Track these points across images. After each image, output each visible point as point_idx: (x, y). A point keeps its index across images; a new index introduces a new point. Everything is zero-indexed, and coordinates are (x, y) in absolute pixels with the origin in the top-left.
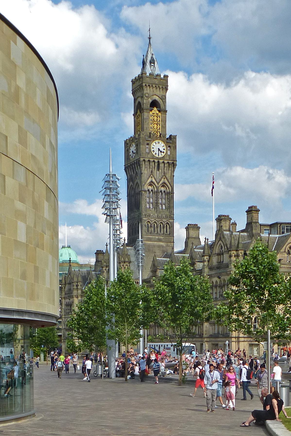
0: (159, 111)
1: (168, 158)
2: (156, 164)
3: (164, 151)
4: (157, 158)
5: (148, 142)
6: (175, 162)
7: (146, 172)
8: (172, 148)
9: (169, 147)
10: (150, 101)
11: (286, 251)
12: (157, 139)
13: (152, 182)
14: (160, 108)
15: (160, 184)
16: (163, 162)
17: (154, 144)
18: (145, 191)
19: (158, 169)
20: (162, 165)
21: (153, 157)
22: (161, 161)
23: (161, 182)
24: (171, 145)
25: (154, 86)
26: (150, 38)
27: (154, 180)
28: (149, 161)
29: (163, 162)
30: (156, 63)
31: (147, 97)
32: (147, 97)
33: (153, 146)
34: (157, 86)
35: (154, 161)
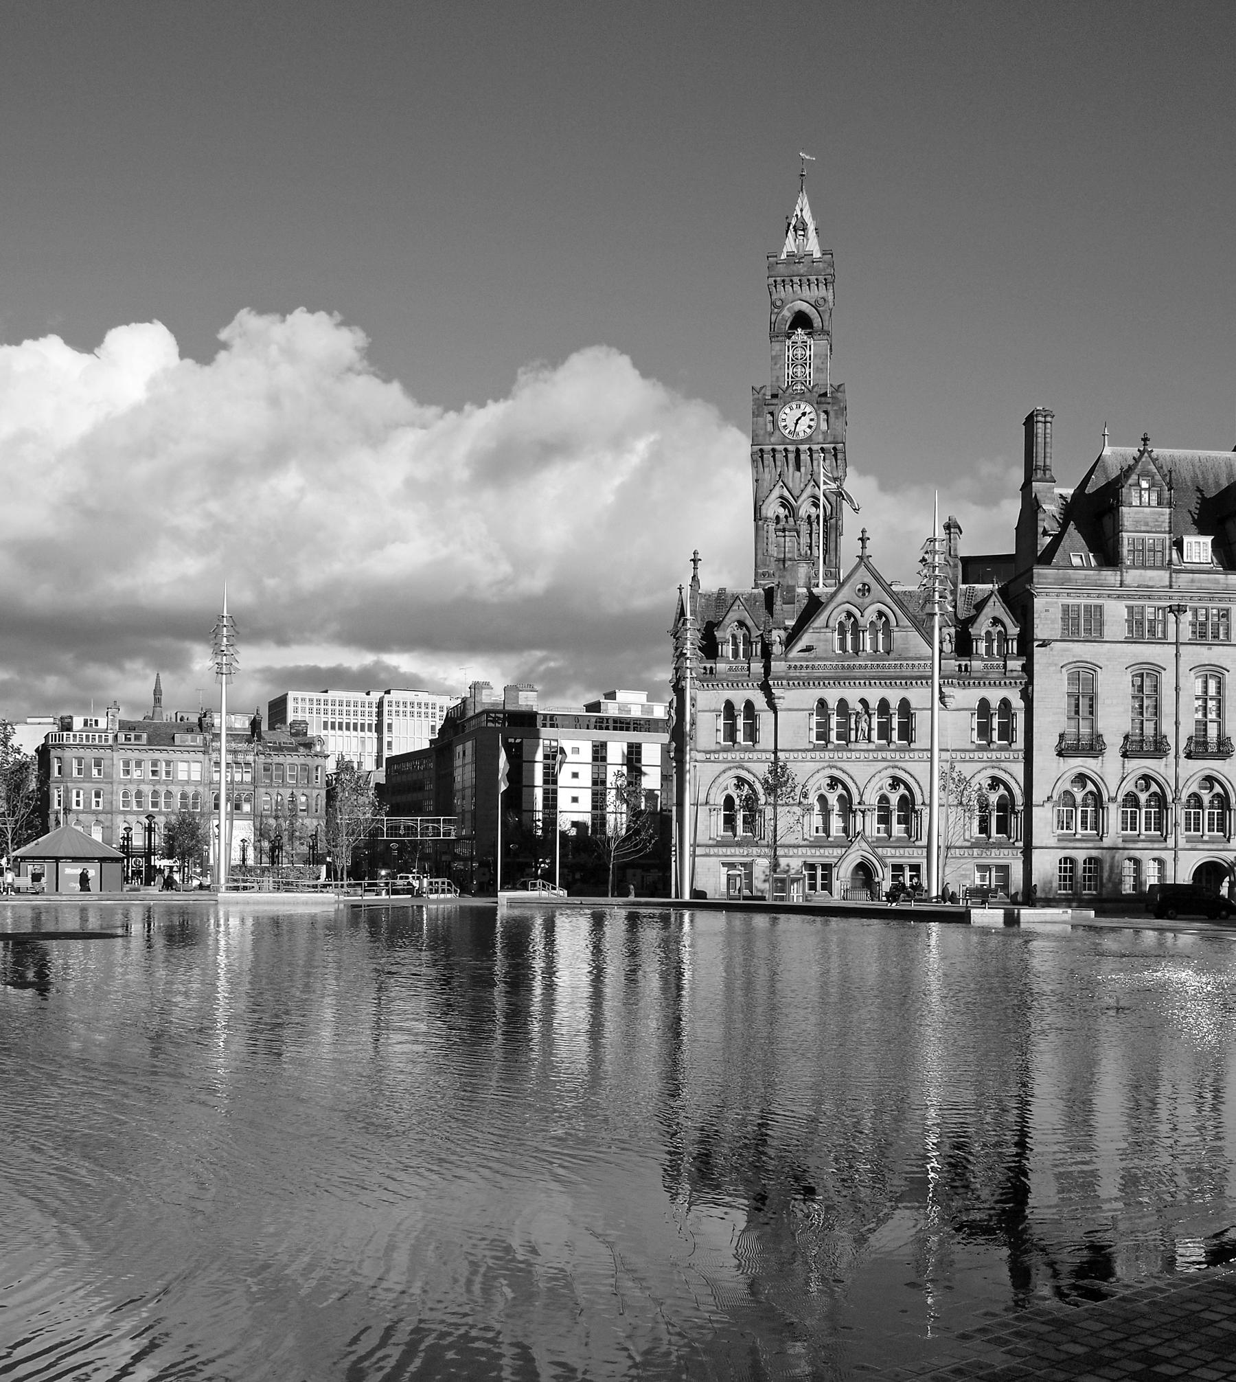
1: (820, 438)
2: (791, 456)
3: (812, 423)
4: (793, 442)
5: (771, 408)
7: (767, 476)
8: (832, 414)
9: (826, 412)
10: (787, 314)
11: (834, 623)
12: (793, 399)
13: (782, 497)
14: (812, 327)
16: (810, 449)
17: (787, 410)
18: (766, 519)
19: (798, 469)
20: (805, 457)
22: (804, 447)
23: (805, 495)
24: (829, 408)
25: (796, 279)
27: (786, 494)
28: (774, 450)
29: (810, 449)
30: (811, 228)
31: (778, 307)
32: (778, 307)
33: (784, 416)
34: (804, 279)
35: (786, 450)
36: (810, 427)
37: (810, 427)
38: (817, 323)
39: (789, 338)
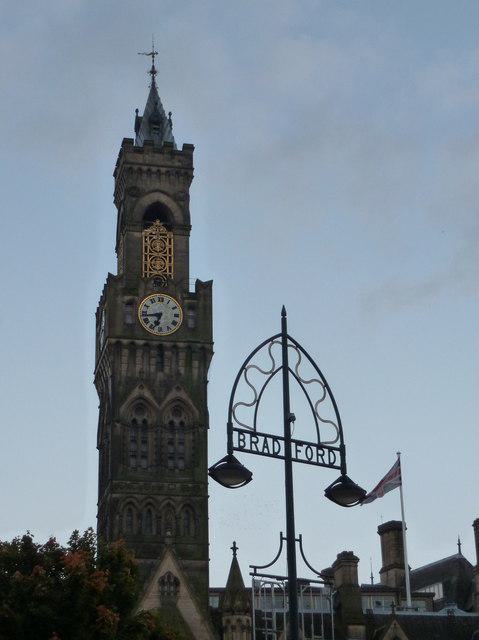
0: (169, 228)
3: (177, 319)
6: (207, 346)
15: (165, 402)
17: (148, 303)
20: (167, 354)
21: (147, 336)
26: (153, 72)
36: (174, 323)
37: (174, 323)
38: (178, 216)
39: (147, 226)
